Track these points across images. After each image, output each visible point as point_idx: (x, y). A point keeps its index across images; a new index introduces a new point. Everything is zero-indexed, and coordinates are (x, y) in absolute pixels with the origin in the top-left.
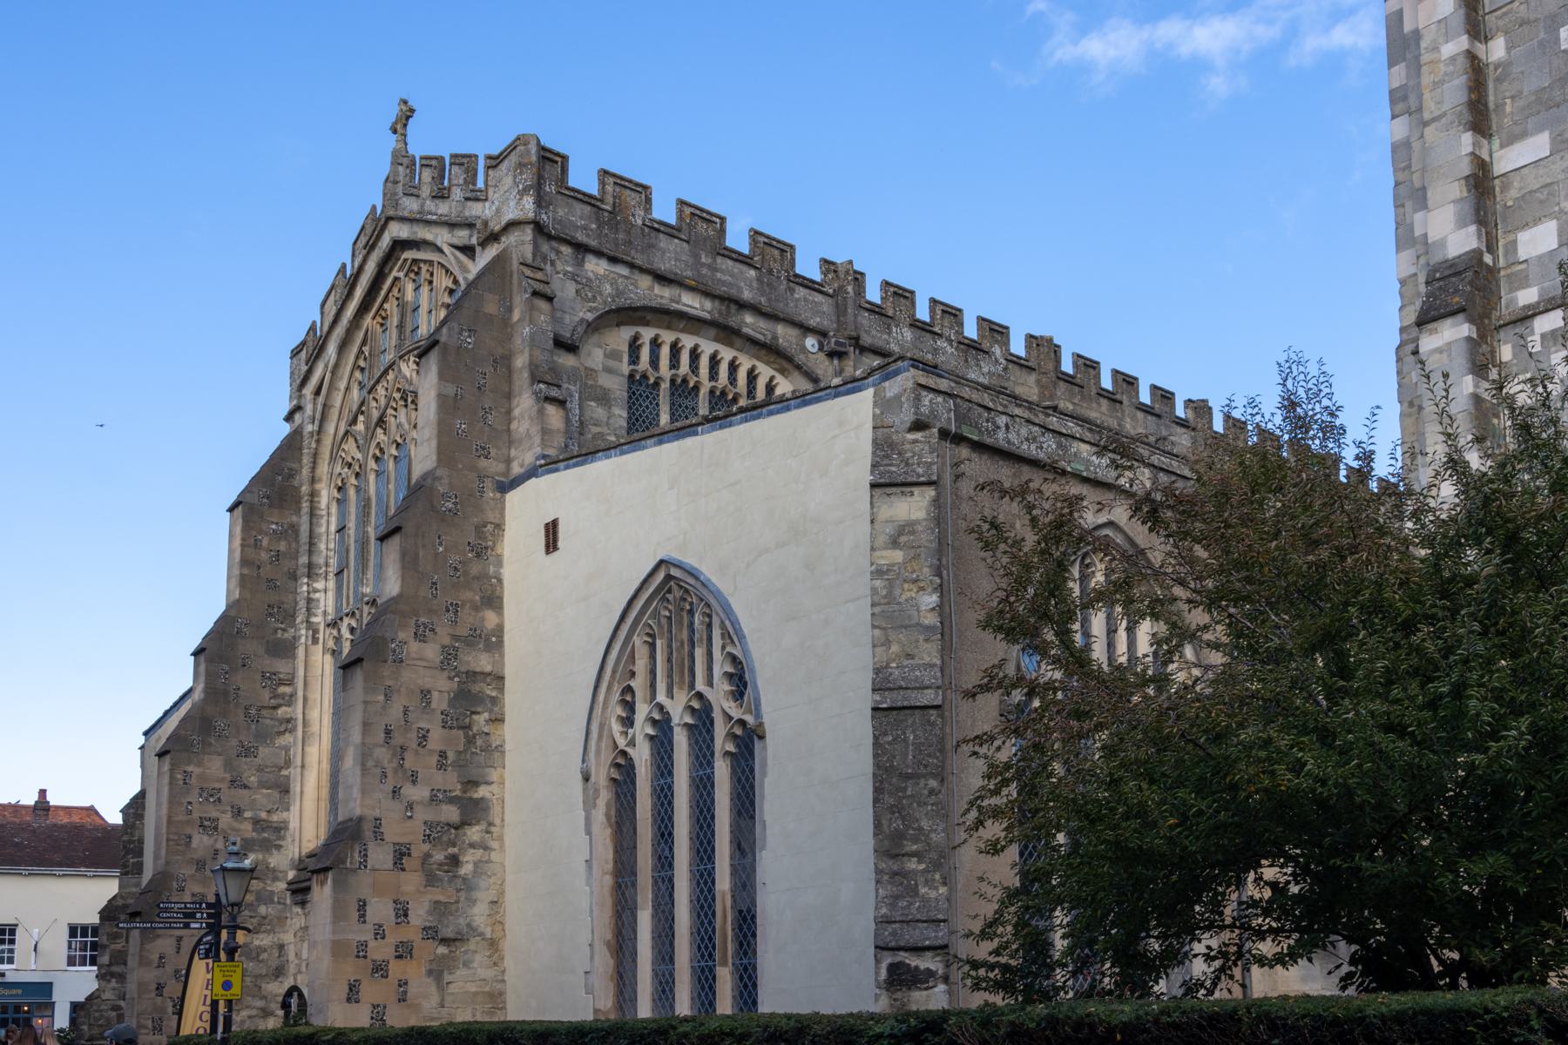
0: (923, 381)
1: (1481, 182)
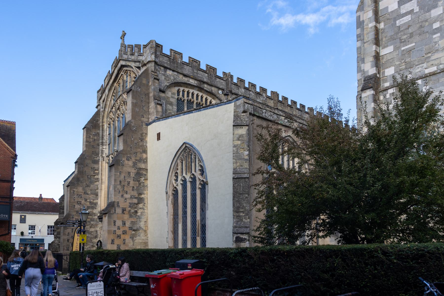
0: (246, 101)
1: (377, 57)
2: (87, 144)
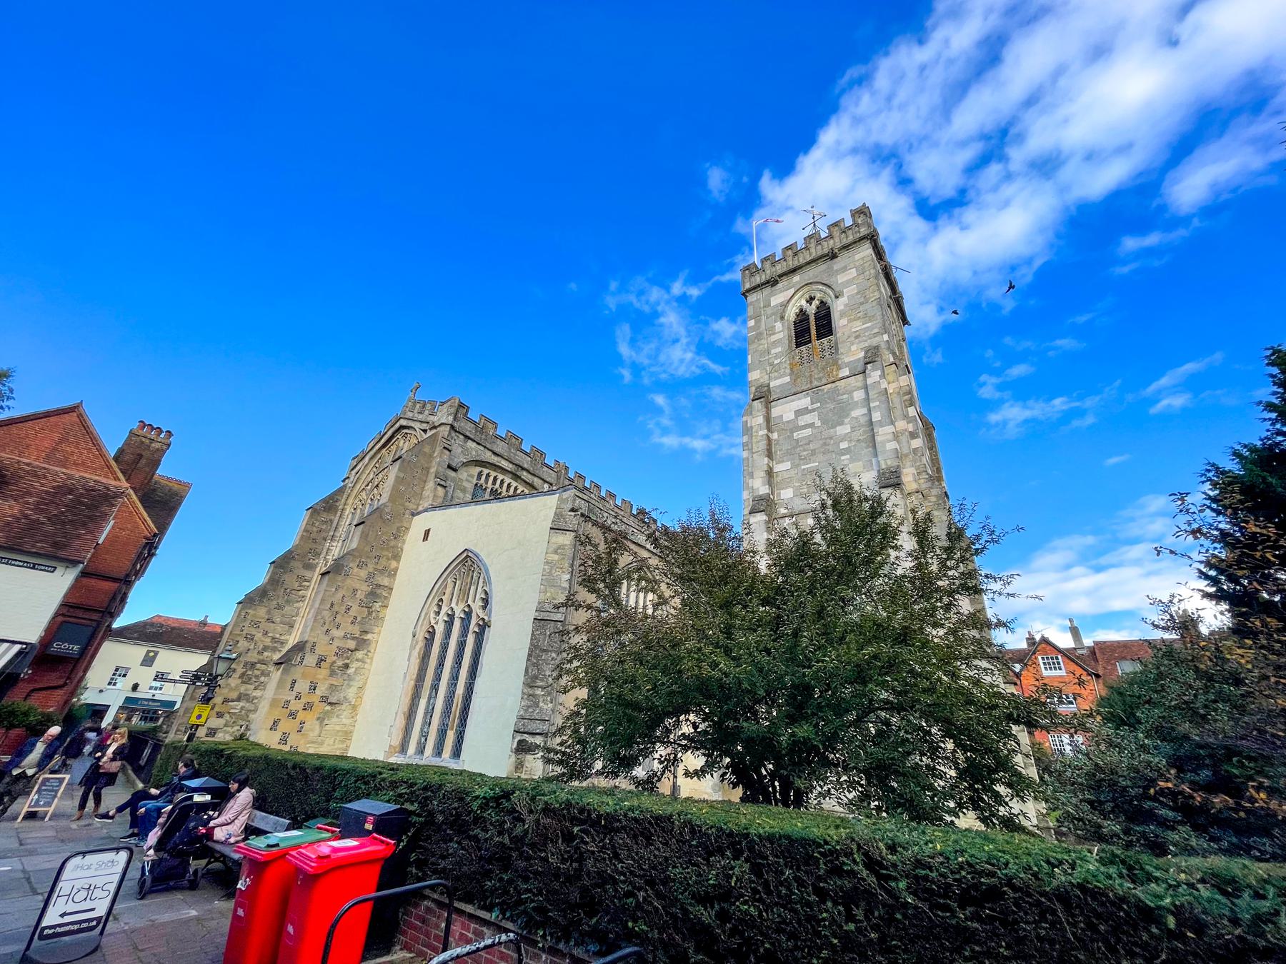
1: (770, 473)
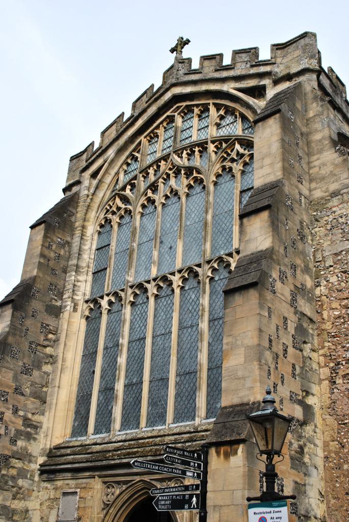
2: (42, 261)
